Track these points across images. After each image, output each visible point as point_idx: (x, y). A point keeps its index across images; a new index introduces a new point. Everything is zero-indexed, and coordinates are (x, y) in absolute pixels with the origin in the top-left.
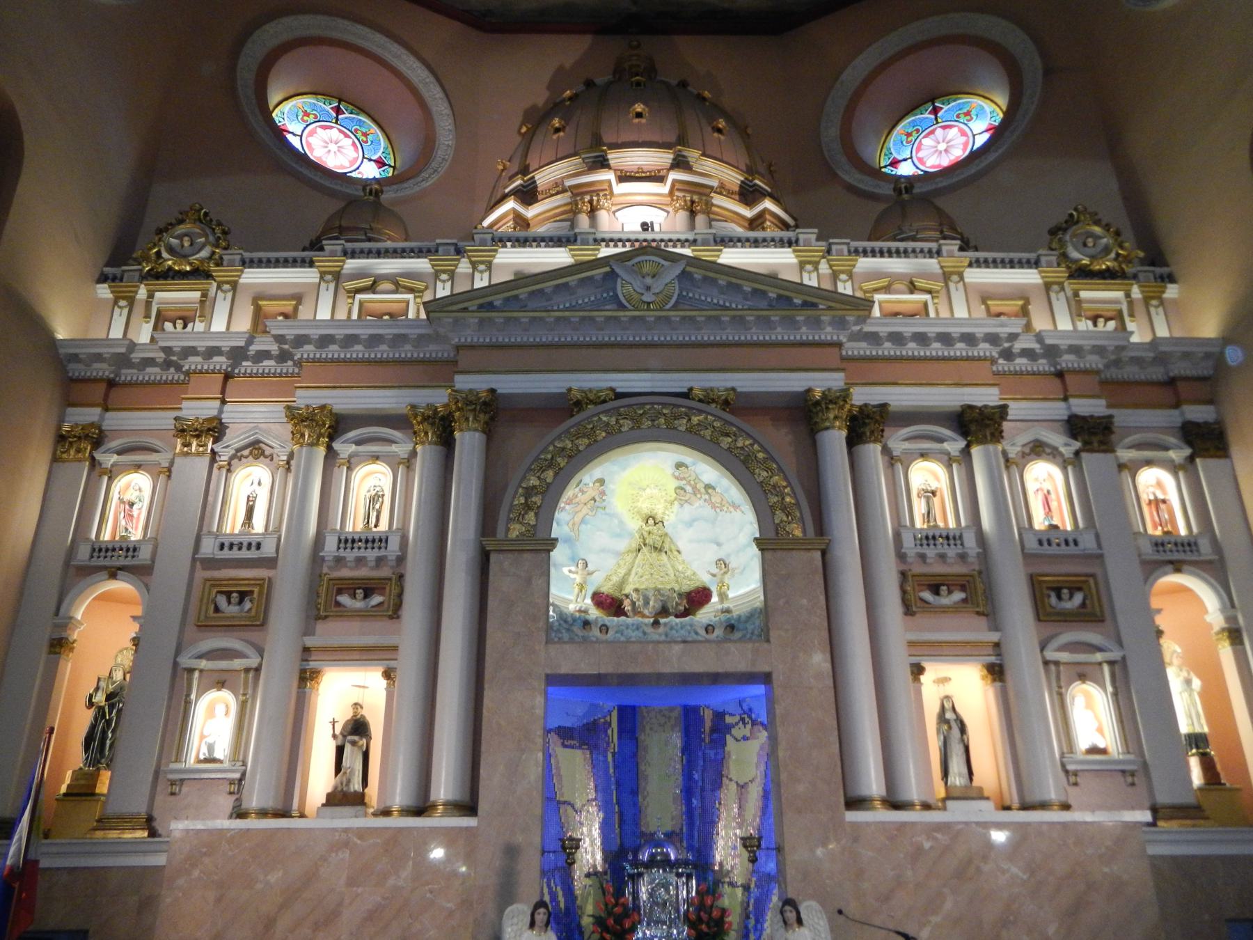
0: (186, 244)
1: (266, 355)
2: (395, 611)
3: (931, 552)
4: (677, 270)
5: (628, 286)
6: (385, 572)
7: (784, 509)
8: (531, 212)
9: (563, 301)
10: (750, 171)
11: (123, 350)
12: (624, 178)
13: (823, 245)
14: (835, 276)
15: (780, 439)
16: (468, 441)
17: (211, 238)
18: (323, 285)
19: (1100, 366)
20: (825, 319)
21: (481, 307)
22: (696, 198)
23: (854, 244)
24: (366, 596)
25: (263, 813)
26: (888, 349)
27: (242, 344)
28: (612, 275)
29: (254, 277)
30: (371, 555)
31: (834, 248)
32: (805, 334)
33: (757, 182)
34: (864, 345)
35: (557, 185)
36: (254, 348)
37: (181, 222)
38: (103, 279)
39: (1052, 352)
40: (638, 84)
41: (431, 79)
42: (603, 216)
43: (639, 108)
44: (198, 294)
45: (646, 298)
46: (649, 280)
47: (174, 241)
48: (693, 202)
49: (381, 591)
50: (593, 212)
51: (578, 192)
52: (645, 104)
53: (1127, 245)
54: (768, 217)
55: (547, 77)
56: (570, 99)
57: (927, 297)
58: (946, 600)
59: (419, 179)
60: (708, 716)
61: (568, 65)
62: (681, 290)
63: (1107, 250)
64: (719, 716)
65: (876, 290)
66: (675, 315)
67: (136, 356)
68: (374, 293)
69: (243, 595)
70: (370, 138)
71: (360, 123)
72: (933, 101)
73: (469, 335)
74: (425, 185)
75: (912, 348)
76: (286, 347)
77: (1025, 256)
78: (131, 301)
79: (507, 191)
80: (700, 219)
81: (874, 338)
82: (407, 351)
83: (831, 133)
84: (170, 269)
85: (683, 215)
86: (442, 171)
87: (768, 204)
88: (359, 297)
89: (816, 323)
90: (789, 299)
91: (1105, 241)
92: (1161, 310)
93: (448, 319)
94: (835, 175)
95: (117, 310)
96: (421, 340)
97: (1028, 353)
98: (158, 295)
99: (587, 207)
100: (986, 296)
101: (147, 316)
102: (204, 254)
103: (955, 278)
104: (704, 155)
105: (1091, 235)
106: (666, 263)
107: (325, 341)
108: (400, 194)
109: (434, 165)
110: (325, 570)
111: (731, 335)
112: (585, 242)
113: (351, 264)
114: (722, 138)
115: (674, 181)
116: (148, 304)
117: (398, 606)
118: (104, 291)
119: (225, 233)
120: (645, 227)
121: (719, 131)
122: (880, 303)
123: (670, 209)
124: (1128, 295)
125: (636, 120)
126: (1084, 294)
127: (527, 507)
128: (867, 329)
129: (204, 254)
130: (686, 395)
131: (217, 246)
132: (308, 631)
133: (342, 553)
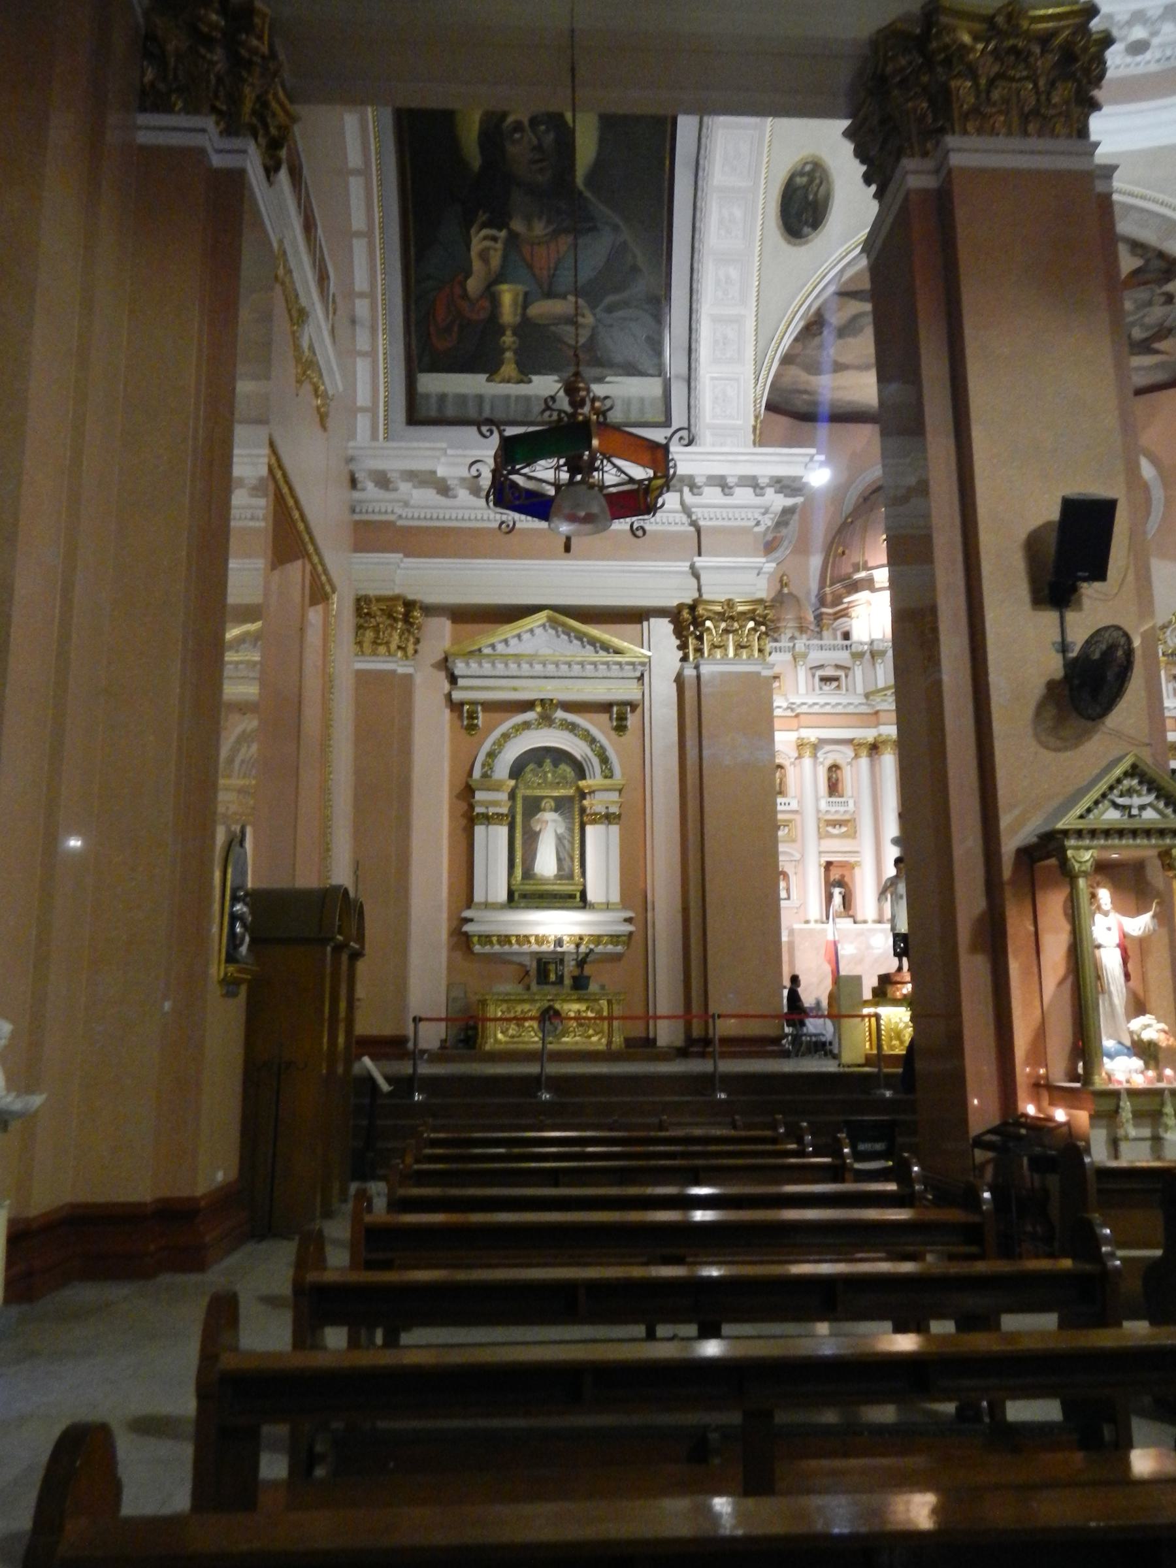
2: (853, 834)
6: (846, 817)
24: (840, 826)
25: (816, 921)
30: (842, 809)
49: (846, 825)
69: (785, 826)
82: (850, 709)
110: (820, 816)
117: (855, 832)
132: (819, 845)
133: (828, 808)
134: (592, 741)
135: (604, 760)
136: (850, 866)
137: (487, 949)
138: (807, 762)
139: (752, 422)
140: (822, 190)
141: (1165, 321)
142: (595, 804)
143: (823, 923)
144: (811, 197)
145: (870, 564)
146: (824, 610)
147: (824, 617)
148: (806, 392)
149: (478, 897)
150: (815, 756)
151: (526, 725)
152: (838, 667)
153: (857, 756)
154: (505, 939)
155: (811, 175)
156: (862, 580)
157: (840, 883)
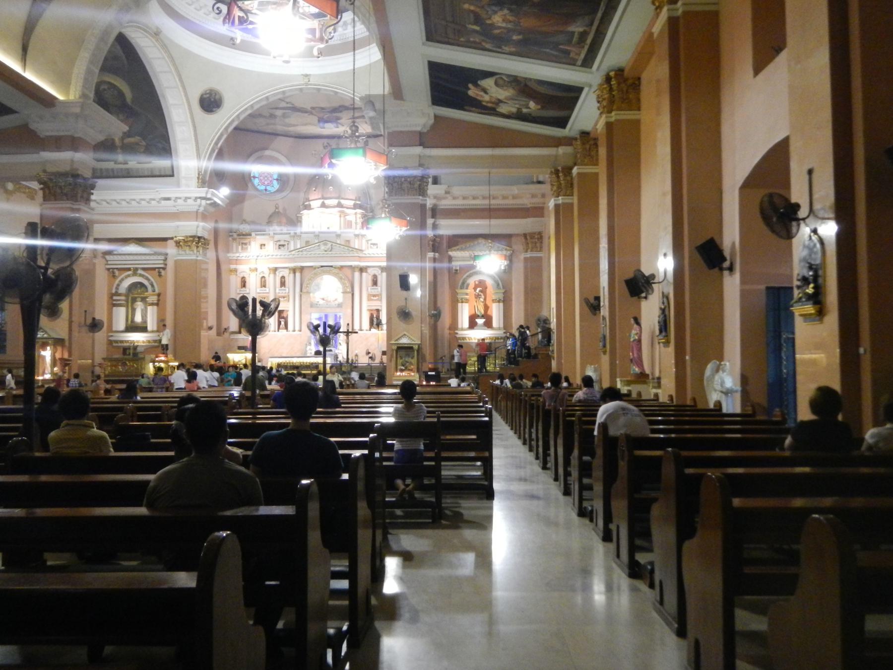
3: (373, 291)
6: (286, 295)
7: (347, 287)
15: (348, 272)
16: (298, 275)
24: (284, 298)
26: (368, 255)
30: (284, 292)
58: (375, 298)
60: (338, 316)
64: (340, 316)
73: (296, 256)
80: (342, 218)
81: (365, 254)
87: (359, 211)
117: (289, 301)
127: (307, 287)
130: (332, 266)
134: (147, 279)
135: (152, 286)
136: (287, 311)
137: (117, 345)
138: (272, 276)
139: (197, 176)
142: (149, 300)
143: (275, 331)
144: (212, 100)
145: (310, 199)
149: (114, 329)
150: (275, 273)
151: (129, 276)
152: (285, 241)
153: (290, 273)
154: (122, 342)
155: (210, 94)
157: (283, 318)
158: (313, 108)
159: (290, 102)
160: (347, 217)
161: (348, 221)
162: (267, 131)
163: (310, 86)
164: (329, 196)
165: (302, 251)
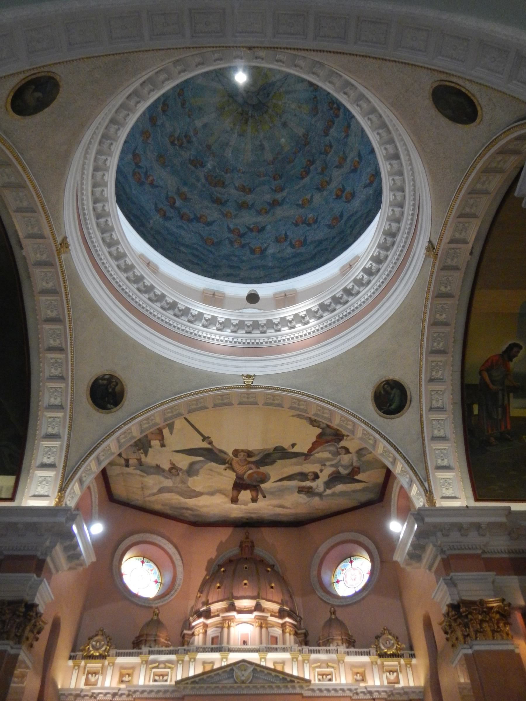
0: (98, 644)
1: (124, 694)
4: (252, 669)
5: (237, 673)
8: (209, 621)
9: (217, 678)
10: (282, 604)
11: (78, 692)
12: (240, 612)
13: (300, 648)
14: (303, 661)
17: (106, 643)
18: (142, 666)
19: (386, 697)
20: (297, 685)
21: (193, 682)
22: (262, 621)
23: (311, 648)
26: (318, 693)
27: (116, 691)
28: (232, 670)
29: (121, 660)
31: (304, 650)
32: (291, 691)
33: (285, 608)
34: (310, 692)
35: (217, 611)
36: (120, 692)
37: (97, 635)
38: (71, 658)
39: (370, 693)
40: (246, 568)
41: (176, 552)
42: (232, 629)
43: (245, 581)
44: (100, 665)
45: (243, 678)
46: (243, 672)
47: (94, 643)
48: (261, 623)
50: (229, 627)
51: (225, 619)
52: (247, 580)
53: (399, 643)
54: (287, 624)
55: (216, 547)
56: (224, 571)
57: (332, 670)
59: (170, 595)
61: (224, 540)
62: (254, 673)
63: (393, 645)
65: (317, 667)
66: (251, 685)
67: (83, 694)
68: (158, 668)
70: (153, 571)
71: (150, 566)
72: (350, 557)
73: (188, 692)
74: (173, 597)
75: (325, 693)
76: (131, 693)
77: (365, 650)
78: (79, 666)
79: (201, 610)
80: (264, 630)
81: (313, 690)
83: (314, 573)
84: (92, 654)
85: (257, 629)
86: (178, 590)
87: (288, 620)
88: (154, 670)
89: (294, 687)
90: (286, 679)
91: (392, 642)
92: (410, 669)
93: (182, 686)
94: (315, 592)
95: (74, 671)
96: (173, 691)
97: (363, 693)
98: (89, 665)
99: (226, 625)
100: (353, 666)
101: (84, 673)
102: (104, 648)
103: (342, 662)
104: (267, 600)
105: (388, 639)
106: (249, 665)
107: (143, 692)
108: (163, 603)
109: (176, 587)
111: (268, 691)
112: (225, 651)
113: (152, 657)
114: (273, 590)
115: (256, 616)
116: (85, 668)
118: (71, 663)
119: (110, 639)
120: (245, 643)
121: (272, 587)
122: (318, 672)
123: (254, 624)
124: (399, 664)
125: (244, 587)
126: (385, 663)
128: (311, 687)
129: (104, 648)
131: (108, 645)
140: (118, 388)
141: (352, 463)
144: (110, 390)
145: (210, 602)
146: (186, 632)
147: (186, 636)
148: (187, 509)
156: (204, 611)
158: (236, 453)
159: (209, 438)
160: (269, 629)
161: (272, 637)
162: (158, 507)
163: (252, 390)
164: (241, 594)
165: (197, 683)
